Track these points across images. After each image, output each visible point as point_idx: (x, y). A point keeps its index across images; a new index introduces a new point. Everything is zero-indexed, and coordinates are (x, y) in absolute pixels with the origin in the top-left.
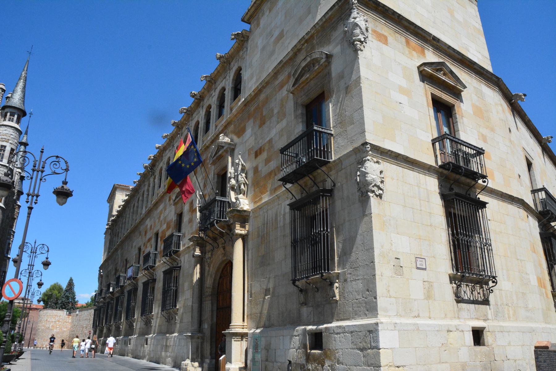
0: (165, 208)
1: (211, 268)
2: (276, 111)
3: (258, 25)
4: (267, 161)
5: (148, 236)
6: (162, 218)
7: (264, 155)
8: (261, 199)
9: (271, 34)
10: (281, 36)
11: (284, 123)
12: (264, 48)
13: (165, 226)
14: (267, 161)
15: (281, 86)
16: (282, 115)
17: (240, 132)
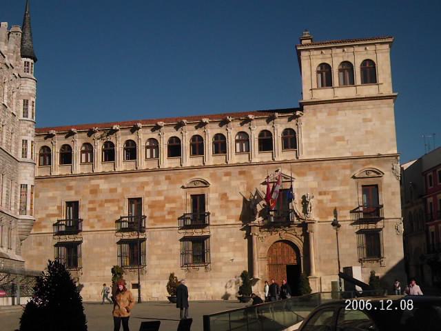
0: (157, 183)
1: (265, 242)
2: (339, 178)
3: (315, 114)
4: (331, 201)
5: (101, 197)
6: (147, 188)
7: (329, 197)
8: (327, 218)
9: (330, 130)
10: (341, 139)
11: (347, 188)
12: (322, 135)
13: (162, 198)
14: (331, 201)
15: (344, 168)
16: (344, 183)
17: (302, 174)
